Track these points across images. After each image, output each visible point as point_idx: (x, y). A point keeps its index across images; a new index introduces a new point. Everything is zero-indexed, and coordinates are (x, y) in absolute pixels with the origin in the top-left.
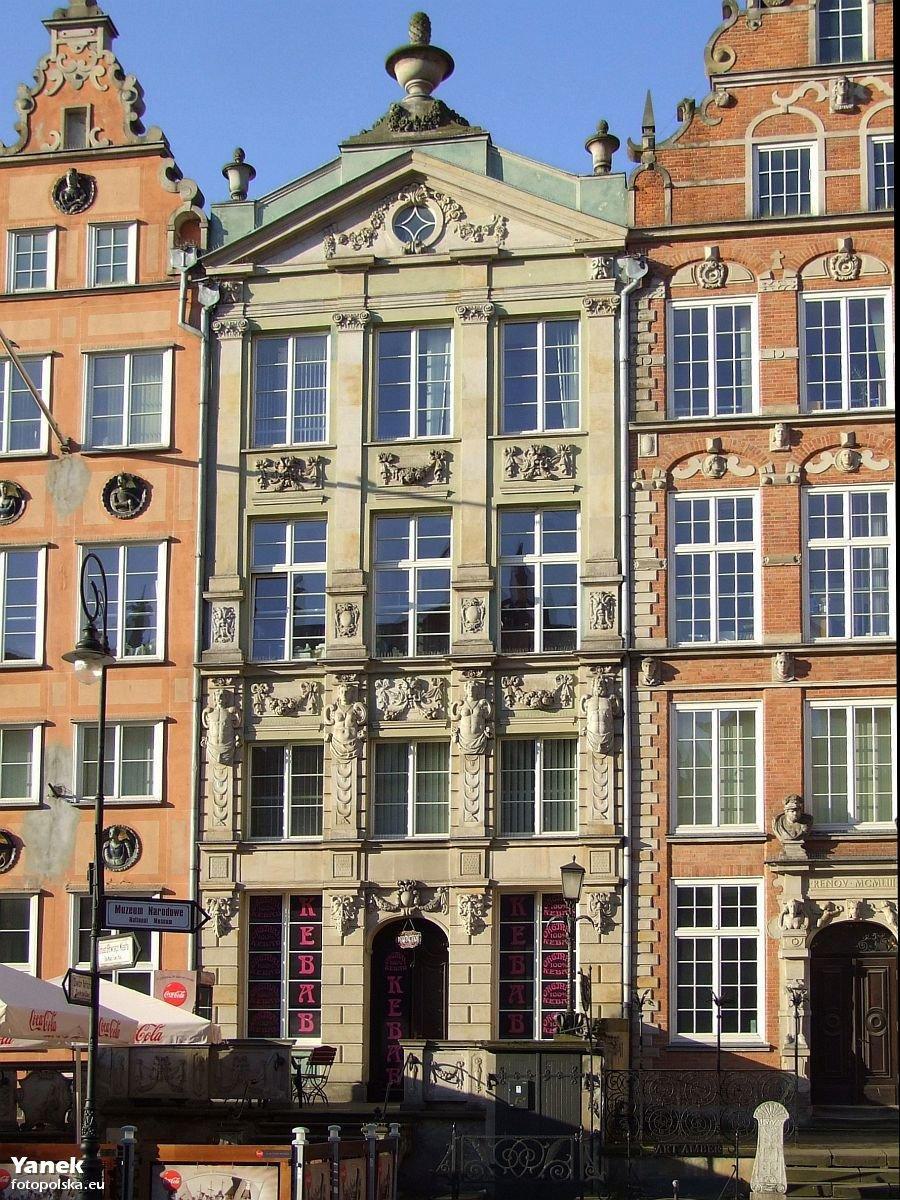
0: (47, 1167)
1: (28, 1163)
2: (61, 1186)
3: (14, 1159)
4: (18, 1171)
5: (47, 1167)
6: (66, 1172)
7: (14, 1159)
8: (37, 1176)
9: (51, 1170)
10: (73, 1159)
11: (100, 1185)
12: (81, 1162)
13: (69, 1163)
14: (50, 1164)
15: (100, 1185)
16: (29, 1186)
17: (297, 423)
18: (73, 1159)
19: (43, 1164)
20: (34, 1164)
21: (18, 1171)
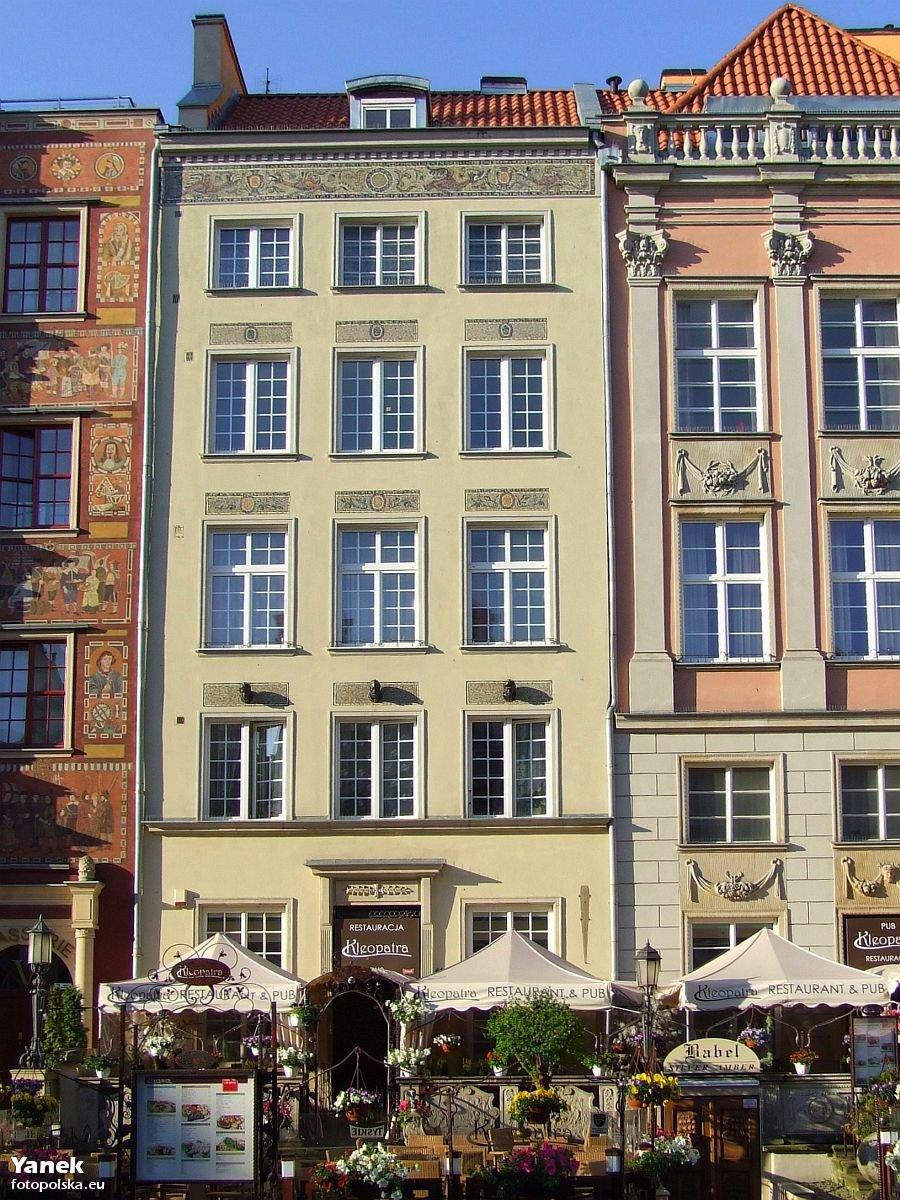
0: (47, 1168)
1: (28, 1163)
2: (61, 1186)
3: (14, 1159)
4: (18, 1171)
5: (47, 1168)
6: (66, 1171)
7: (14, 1159)
8: (37, 1177)
9: (51, 1171)
10: (73, 1159)
11: (100, 1185)
12: (80, 1163)
13: (69, 1163)
14: (51, 1164)
15: (100, 1185)
16: (29, 1186)
17: (731, 615)
18: (73, 1159)
19: (43, 1164)
20: (34, 1164)
21: (18, 1171)
